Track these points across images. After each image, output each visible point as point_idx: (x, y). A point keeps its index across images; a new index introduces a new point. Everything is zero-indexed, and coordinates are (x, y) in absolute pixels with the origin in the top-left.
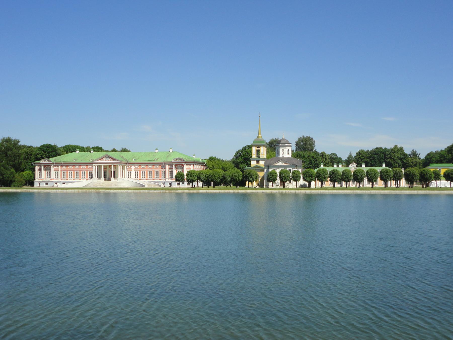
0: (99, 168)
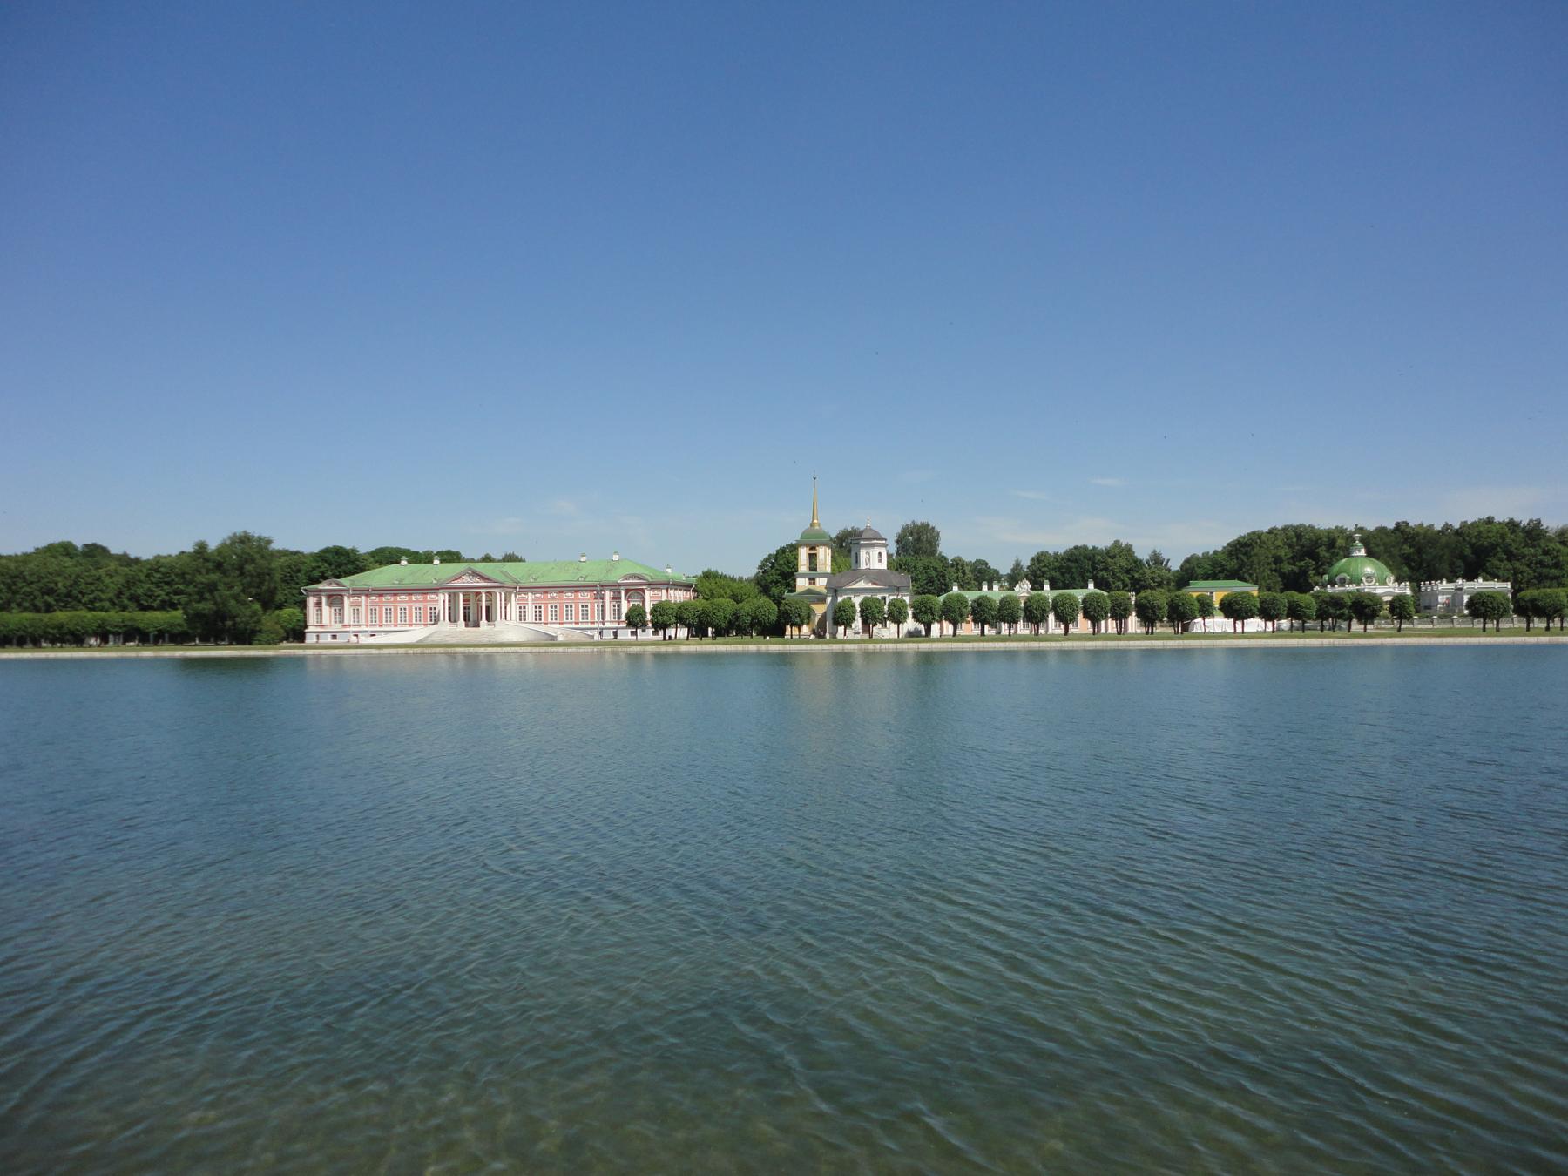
0: (453, 598)
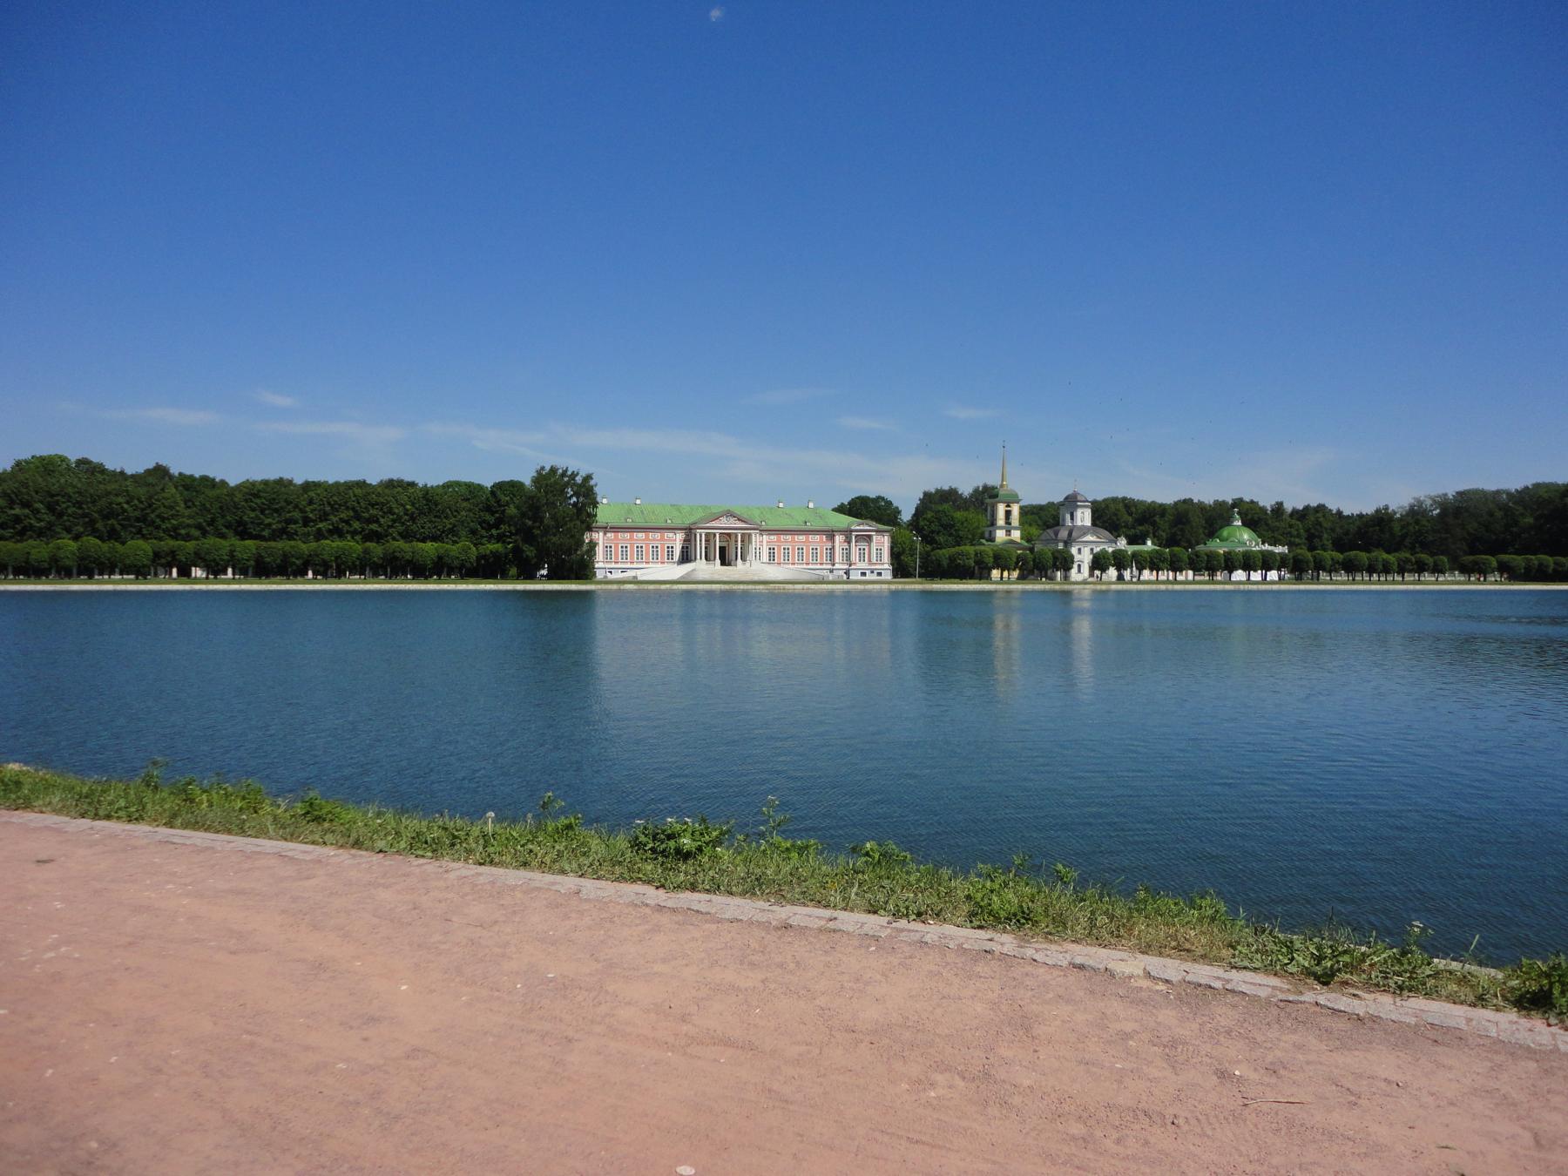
0: (709, 538)
